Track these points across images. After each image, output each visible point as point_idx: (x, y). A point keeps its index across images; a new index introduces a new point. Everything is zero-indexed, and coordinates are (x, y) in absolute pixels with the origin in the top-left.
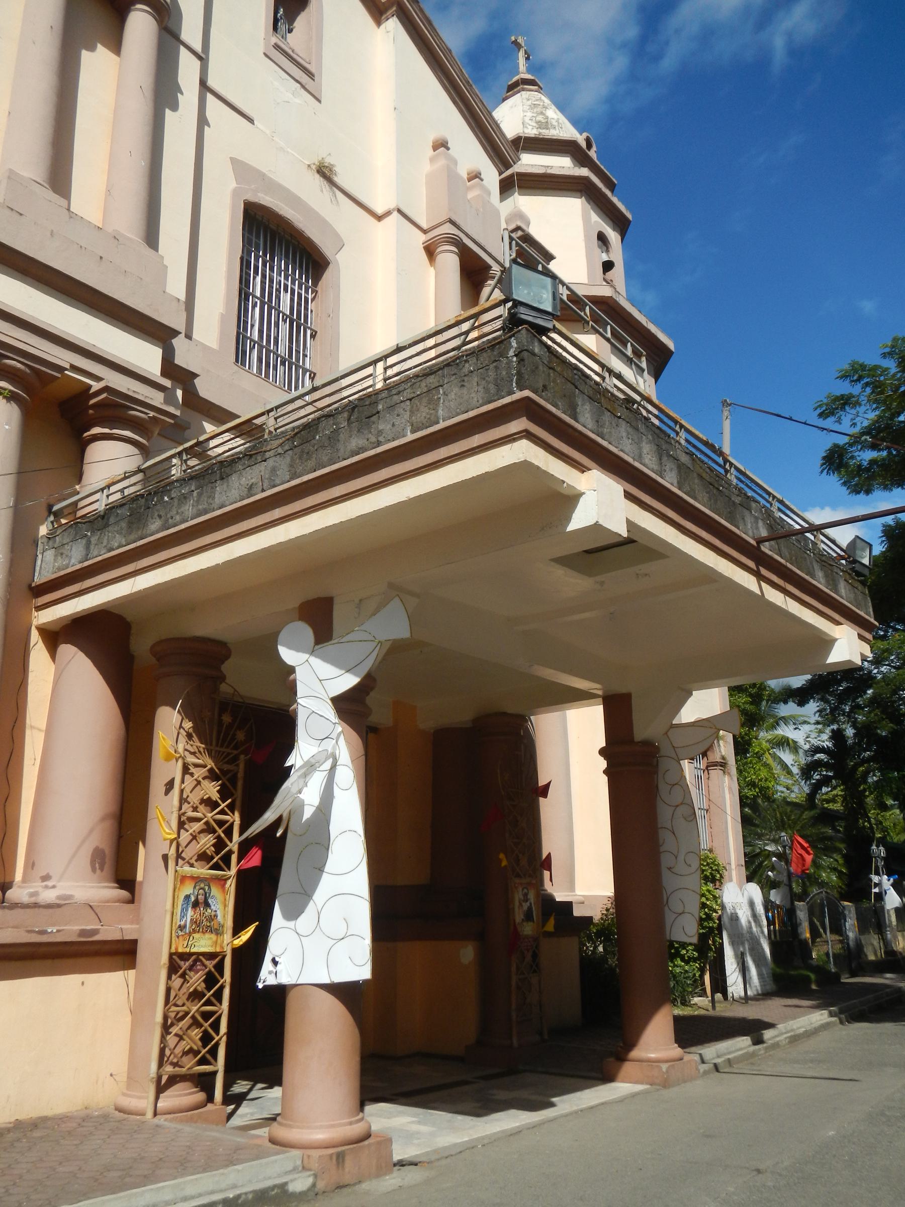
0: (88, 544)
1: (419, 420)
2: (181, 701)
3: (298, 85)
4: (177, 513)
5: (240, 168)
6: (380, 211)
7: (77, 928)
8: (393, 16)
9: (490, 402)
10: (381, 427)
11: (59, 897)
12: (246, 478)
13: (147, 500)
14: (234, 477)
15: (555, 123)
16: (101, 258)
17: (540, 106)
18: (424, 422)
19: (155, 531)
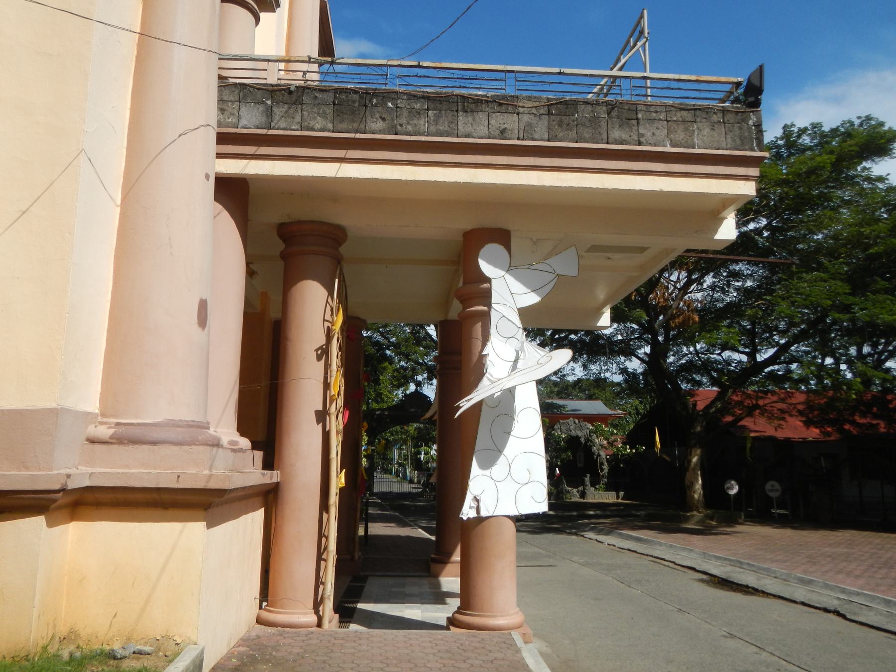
0: (269, 113)
1: (677, 139)
2: (337, 280)
4: (408, 123)
9: (737, 149)
10: (642, 131)
12: (496, 121)
13: (361, 97)
14: (482, 116)
18: (683, 142)
19: (376, 129)
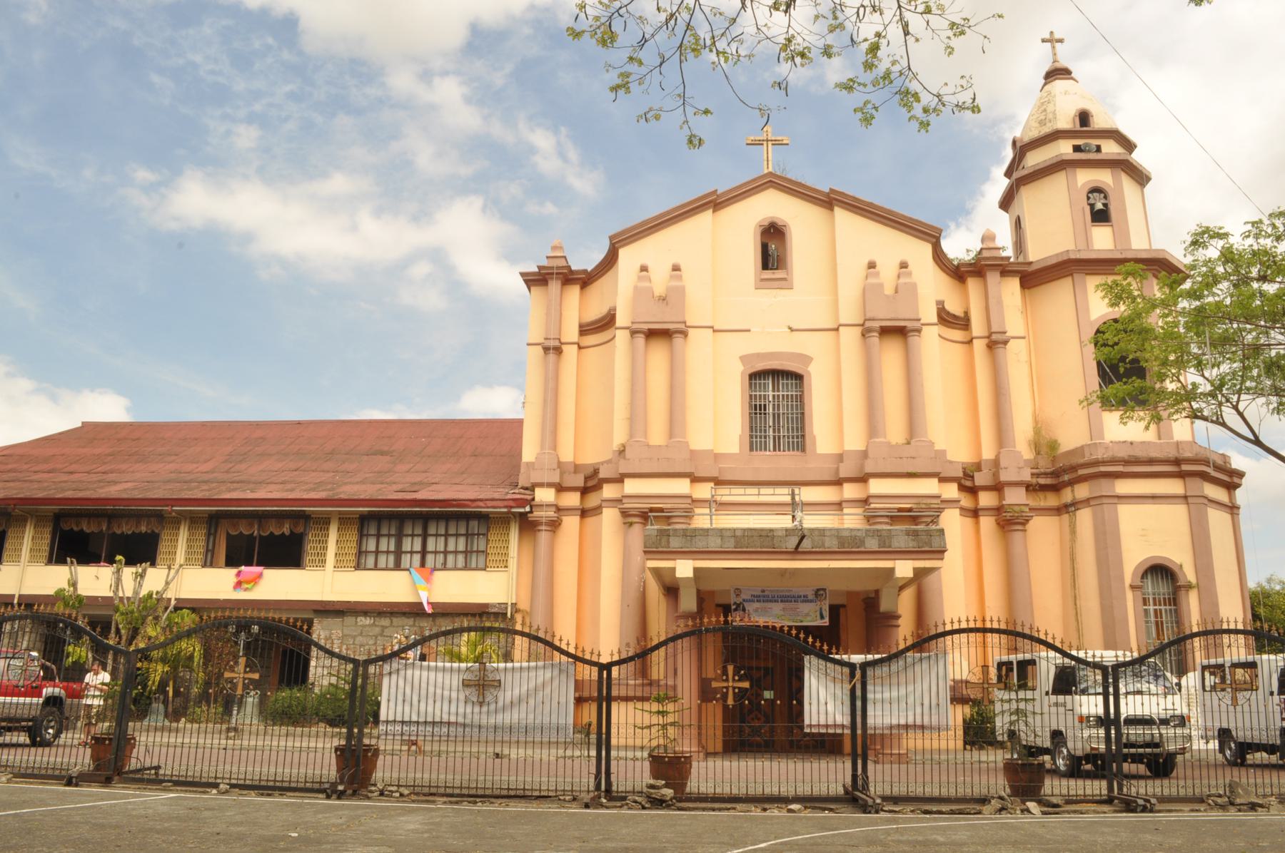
5: (744, 359)
15: (1050, 116)
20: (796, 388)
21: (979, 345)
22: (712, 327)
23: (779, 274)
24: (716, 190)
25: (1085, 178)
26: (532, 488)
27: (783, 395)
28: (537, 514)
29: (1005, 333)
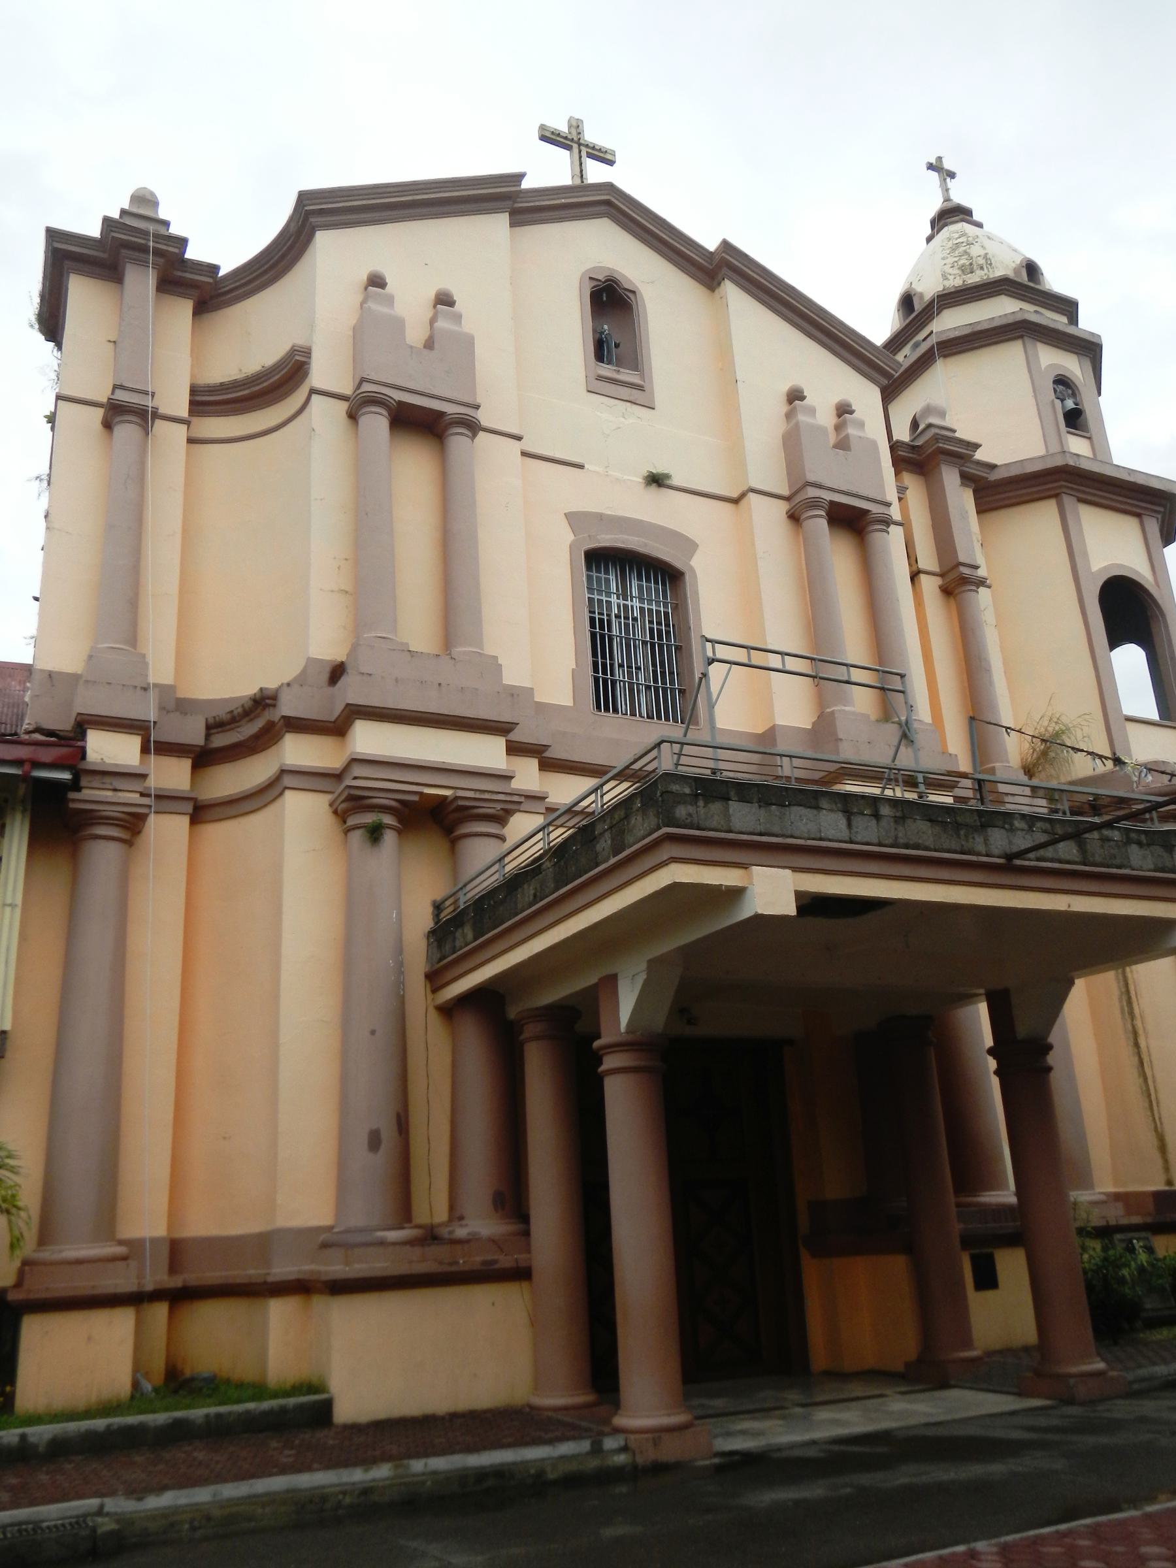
3: (629, 404)
5: (574, 519)
6: (735, 494)
7: (479, 1259)
8: (724, 279)
11: (469, 1234)
15: (981, 261)
16: (440, 684)
17: (965, 244)
20: (665, 597)
21: (929, 585)
22: (519, 438)
23: (626, 375)
24: (520, 177)
25: (1051, 359)
26: (82, 725)
27: (642, 609)
28: (92, 794)
29: (977, 567)
